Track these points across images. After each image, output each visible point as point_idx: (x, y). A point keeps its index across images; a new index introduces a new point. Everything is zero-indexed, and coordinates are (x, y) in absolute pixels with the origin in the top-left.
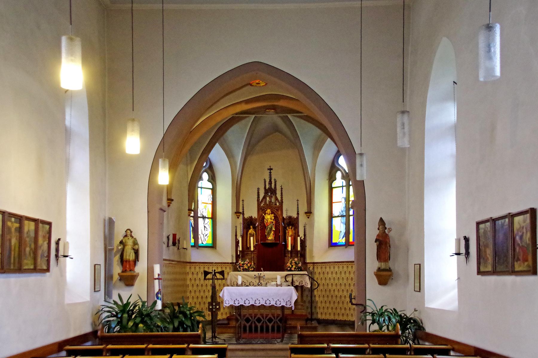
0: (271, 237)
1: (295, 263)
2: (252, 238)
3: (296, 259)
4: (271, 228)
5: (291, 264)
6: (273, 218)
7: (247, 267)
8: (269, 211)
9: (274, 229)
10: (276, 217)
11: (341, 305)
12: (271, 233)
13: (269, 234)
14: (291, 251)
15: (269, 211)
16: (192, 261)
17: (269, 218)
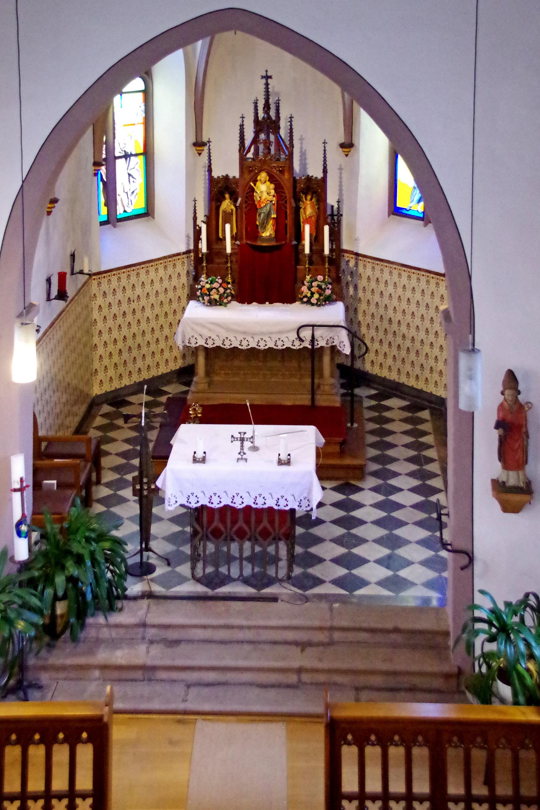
0: (268, 232)
1: (319, 287)
2: (228, 227)
3: (320, 278)
4: (269, 214)
5: (309, 290)
6: (273, 192)
7: (217, 297)
8: (263, 176)
9: (274, 216)
10: (278, 189)
11: (412, 356)
12: (267, 222)
13: (264, 226)
14: (310, 256)
15: (263, 176)
16: (103, 269)
17: (264, 190)
